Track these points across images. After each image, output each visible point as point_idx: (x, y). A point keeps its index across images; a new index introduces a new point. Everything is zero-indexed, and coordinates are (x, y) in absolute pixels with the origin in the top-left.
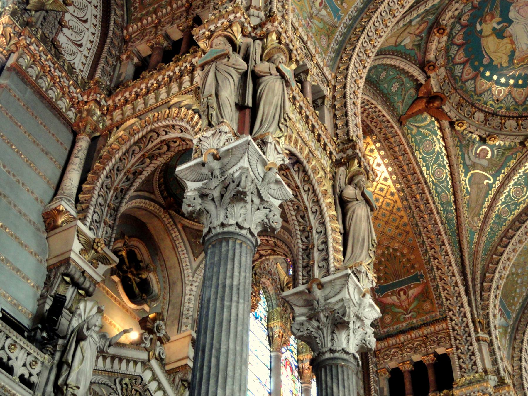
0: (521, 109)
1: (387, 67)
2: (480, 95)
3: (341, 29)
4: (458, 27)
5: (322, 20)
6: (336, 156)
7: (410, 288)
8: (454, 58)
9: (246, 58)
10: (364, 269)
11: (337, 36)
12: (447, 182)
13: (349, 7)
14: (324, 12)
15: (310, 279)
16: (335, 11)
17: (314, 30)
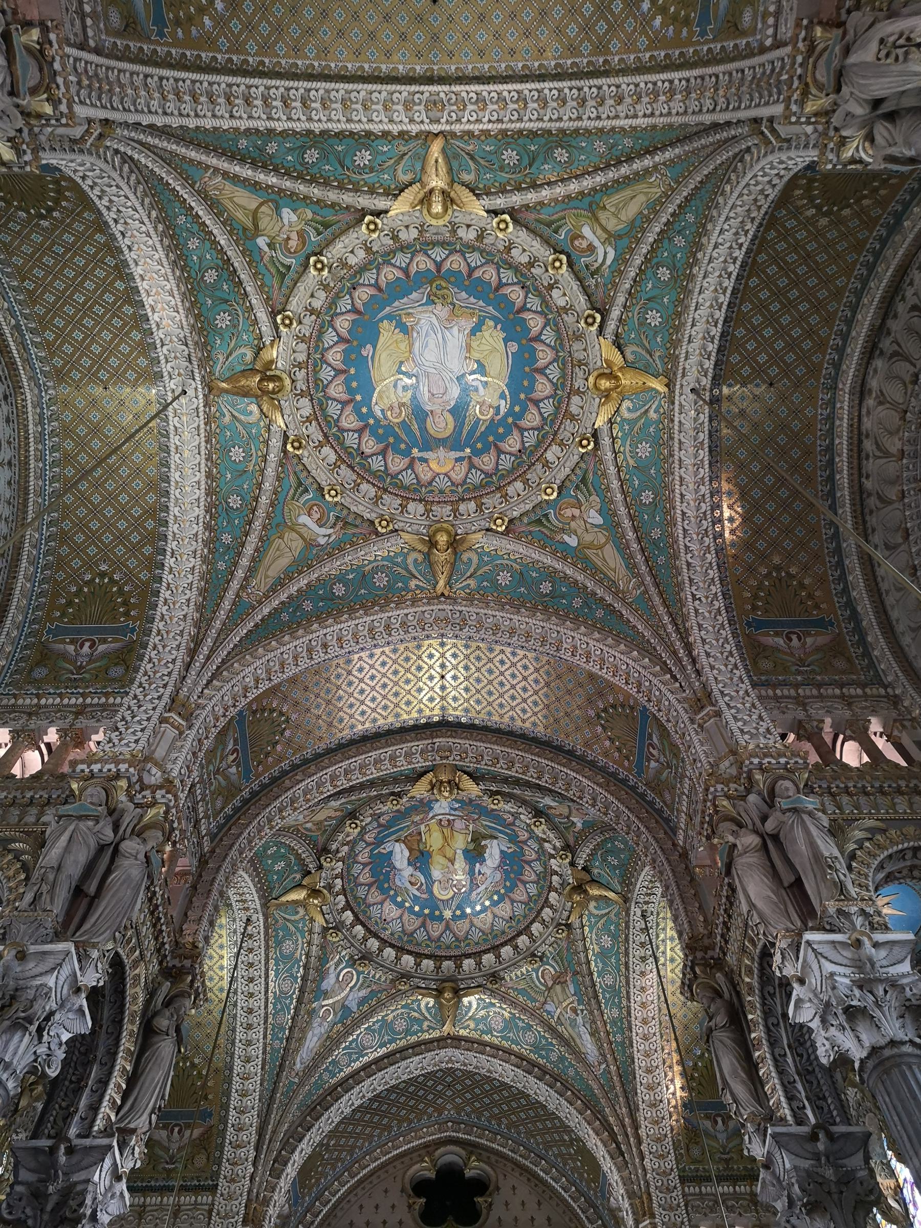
0: (405, 939)
1: (279, 844)
2: (369, 906)
3: (245, 793)
4: (375, 824)
5: (226, 778)
6: (170, 962)
7: (188, 1126)
8: (357, 855)
9: (116, 827)
10: (133, 1143)
11: (237, 801)
12: (292, 999)
13: (264, 772)
14: (233, 770)
15: (60, 1136)
16: (247, 771)
17: (213, 788)
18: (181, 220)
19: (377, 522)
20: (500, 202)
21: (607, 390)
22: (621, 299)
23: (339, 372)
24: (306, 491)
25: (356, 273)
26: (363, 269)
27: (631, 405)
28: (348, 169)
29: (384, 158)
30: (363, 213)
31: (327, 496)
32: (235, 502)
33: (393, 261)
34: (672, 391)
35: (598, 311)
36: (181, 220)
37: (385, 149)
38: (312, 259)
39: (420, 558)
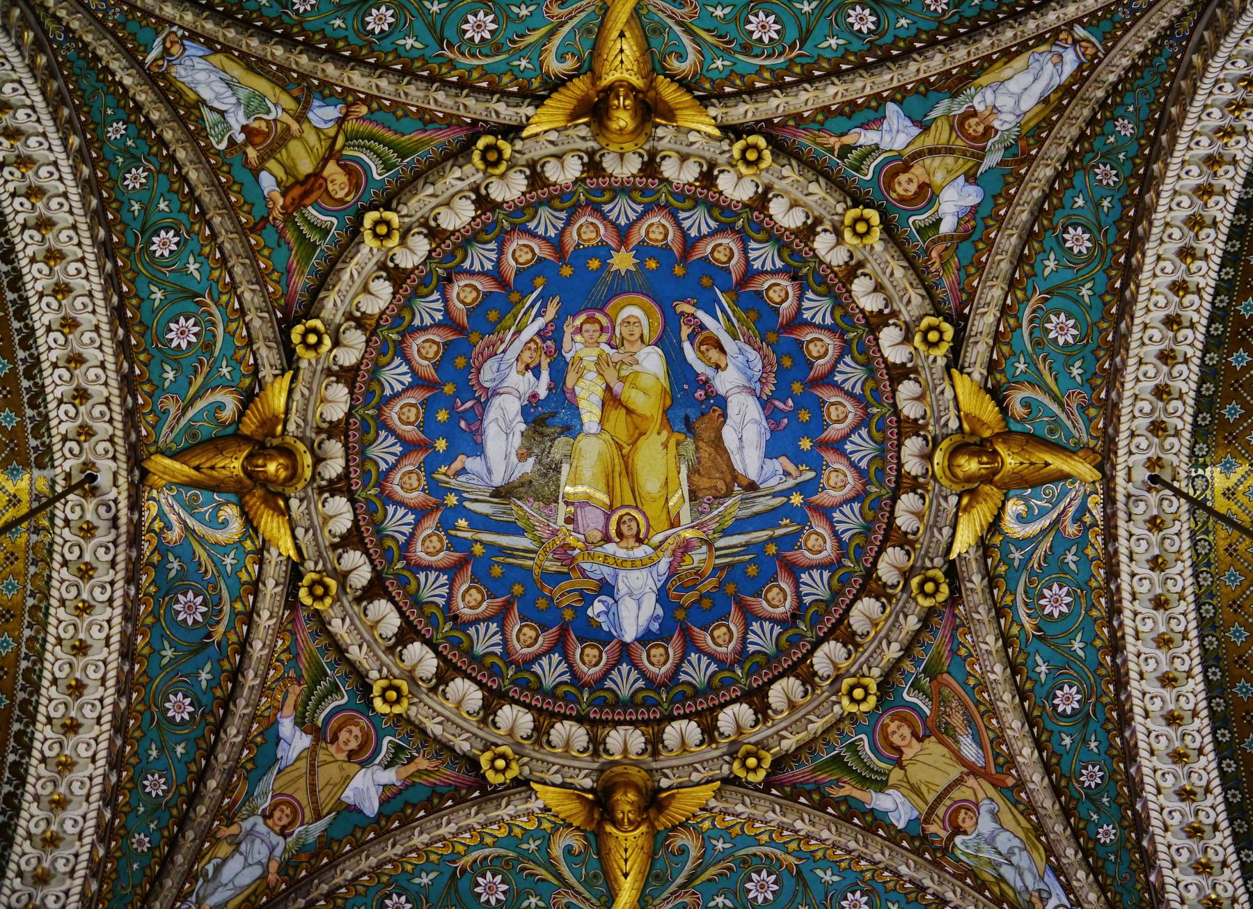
18: (116, 131)
19: (484, 760)
20: (741, 112)
21: (969, 479)
22: (995, 293)
23: (410, 447)
24: (335, 689)
25: (457, 247)
26: (470, 238)
27: (1021, 508)
28: (450, 45)
29: (520, 28)
30: (476, 129)
31: (378, 703)
32: (179, 708)
33: (531, 225)
34: (1108, 481)
35: (947, 319)
36: (116, 131)
37: (524, 12)
38: (370, 218)
39: (577, 842)
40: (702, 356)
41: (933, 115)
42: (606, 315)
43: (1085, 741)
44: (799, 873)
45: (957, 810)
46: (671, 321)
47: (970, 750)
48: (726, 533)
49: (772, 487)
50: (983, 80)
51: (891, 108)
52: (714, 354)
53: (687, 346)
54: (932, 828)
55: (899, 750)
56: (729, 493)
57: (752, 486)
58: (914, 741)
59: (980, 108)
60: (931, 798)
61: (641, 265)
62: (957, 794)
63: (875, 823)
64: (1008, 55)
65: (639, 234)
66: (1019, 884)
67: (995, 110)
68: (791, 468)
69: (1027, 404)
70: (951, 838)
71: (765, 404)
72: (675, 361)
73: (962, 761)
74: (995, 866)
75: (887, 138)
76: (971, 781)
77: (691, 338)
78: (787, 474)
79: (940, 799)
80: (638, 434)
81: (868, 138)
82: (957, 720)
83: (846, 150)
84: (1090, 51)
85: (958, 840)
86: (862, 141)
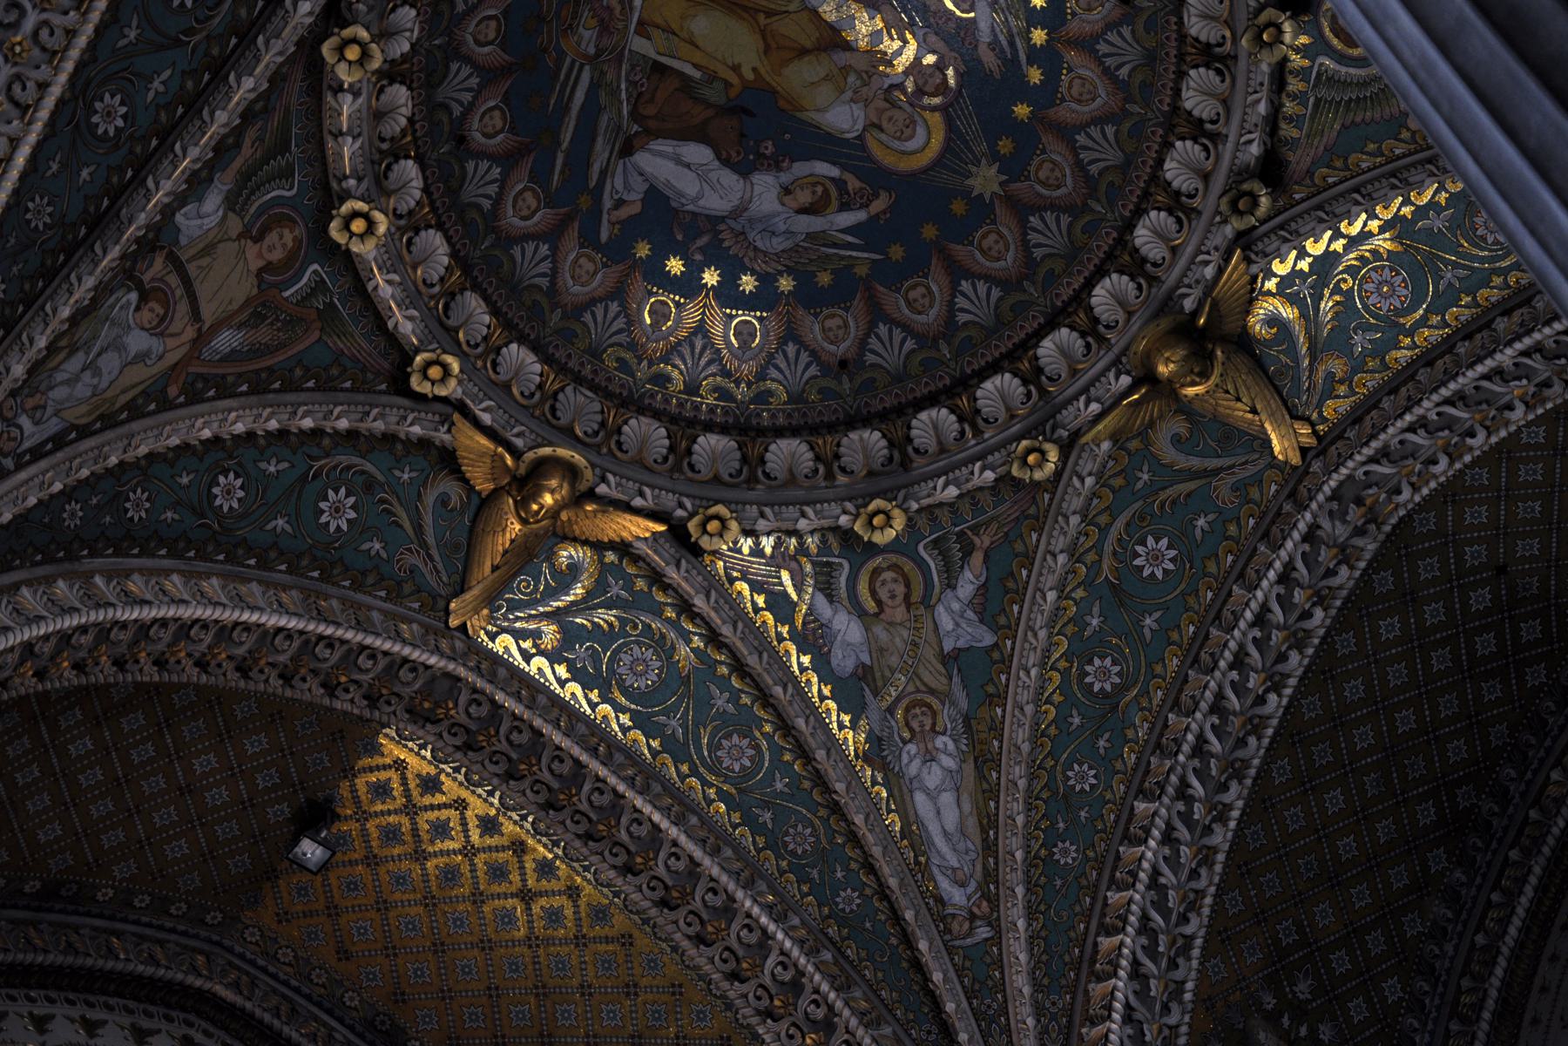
27: (455, 501)
40: (815, 181)
41: (956, 679)
42: (934, 109)
43: (175, 506)
44: (178, 43)
45: (166, 304)
46: (878, 177)
47: (227, 340)
48: (594, 87)
49: (613, 176)
50: (969, 768)
51: (988, 639)
52: (804, 197)
53: (835, 172)
54: (159, 261)
55: (258, 239)
56: (635, 115)
57: (627, 150)
58: (261, 263)
59: (940, 741)
60: (192, 269)
61: (966, 194)
62: (183, 308)
63: (197, 183)
64: (988, 823)
65: (1007, 226)
66: (60, 377)
67: (930, 758)
68: (624, 213)
69: (574, 570)
70: (140, 287)
71: (714, 221)
72: (826, 145)
73: (216, 328)
74: (88, 346)
75: (956, 606)
76: (190, 333)
77: (840, 183)
78: (620, 203)
79: (187, 282)
80: (770, 44)
81: (967, 584)
82: (264, 334)
83: (968, 551)
84: (955, 926)
85: (133, 296)
86: (968, 575)
